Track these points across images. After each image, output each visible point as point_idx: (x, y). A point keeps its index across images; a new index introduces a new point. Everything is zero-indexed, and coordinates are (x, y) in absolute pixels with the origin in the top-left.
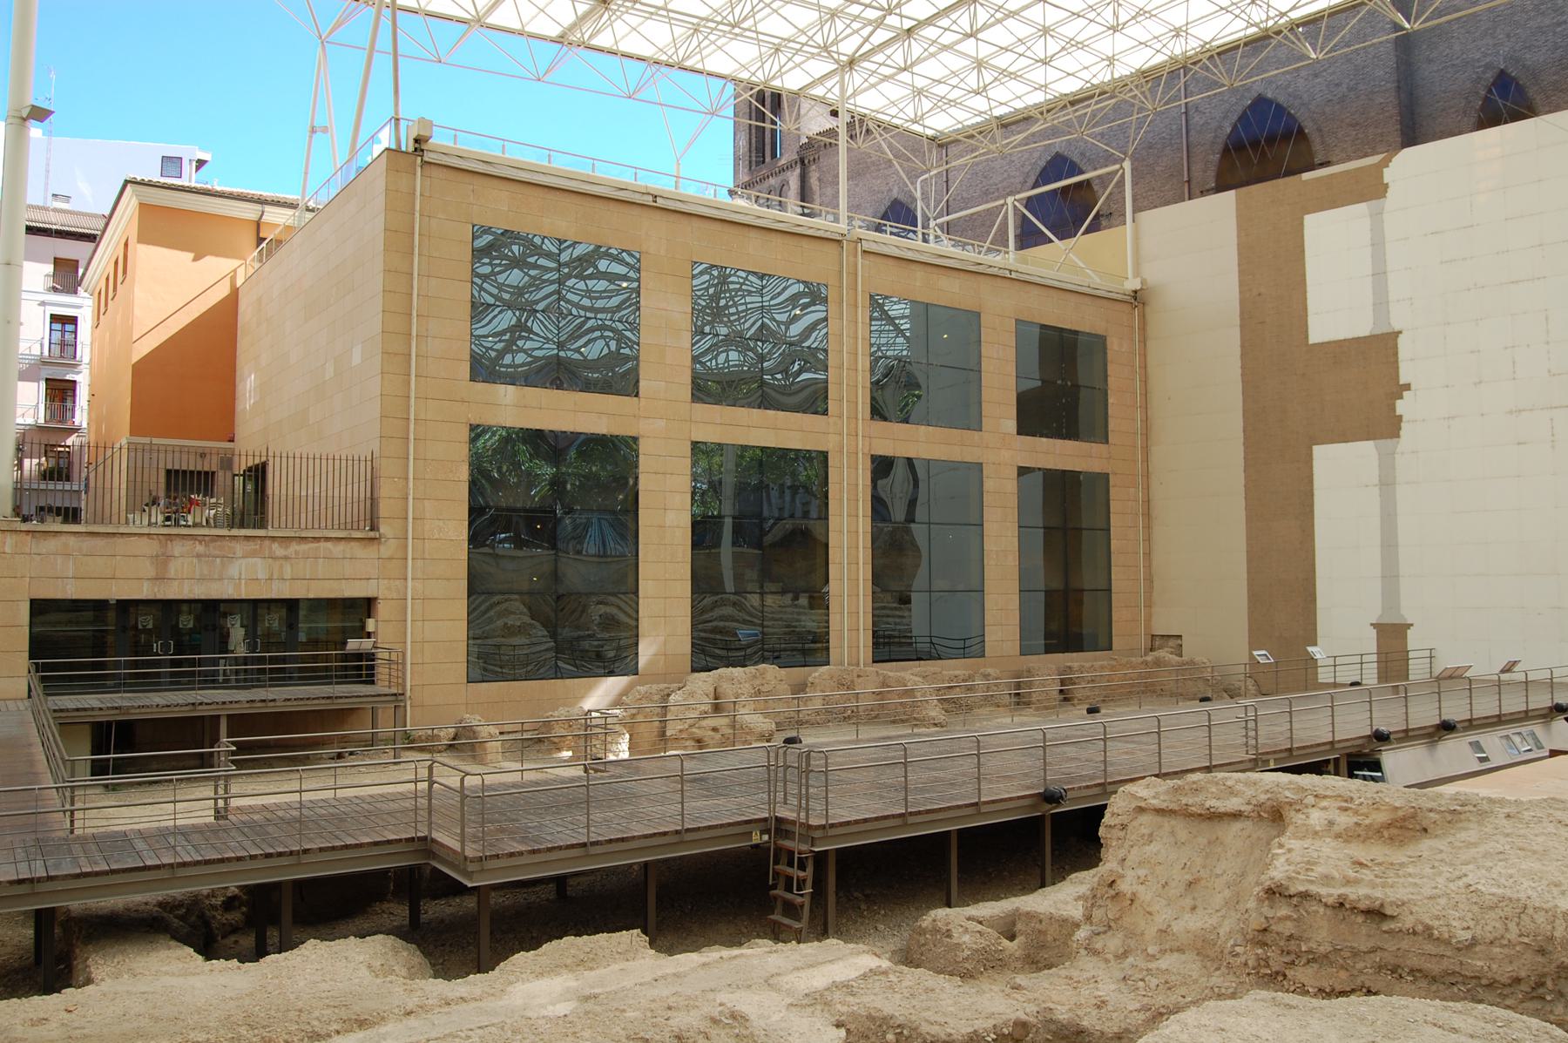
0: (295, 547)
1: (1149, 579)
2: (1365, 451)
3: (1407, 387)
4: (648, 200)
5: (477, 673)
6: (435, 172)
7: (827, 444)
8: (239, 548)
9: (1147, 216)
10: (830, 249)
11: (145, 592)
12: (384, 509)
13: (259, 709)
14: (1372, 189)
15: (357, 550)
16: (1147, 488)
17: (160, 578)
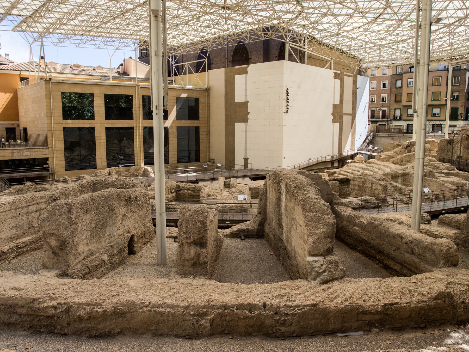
0: (34, 150)
1: (209, 147)
2: (243, 124)
3: (249, 113)
4: (95, 83)
5: (68, 168)
6: (54, 83)
7: (134, 125)
8: (25, 151)
9: (209, 71)
10: (134, 88)
11: (10, 158)
12: (49, 143)
13: (30, 176)
14: (245, 72)
15: (44, 150)
16: (209, 129)
17: (13, 156)
